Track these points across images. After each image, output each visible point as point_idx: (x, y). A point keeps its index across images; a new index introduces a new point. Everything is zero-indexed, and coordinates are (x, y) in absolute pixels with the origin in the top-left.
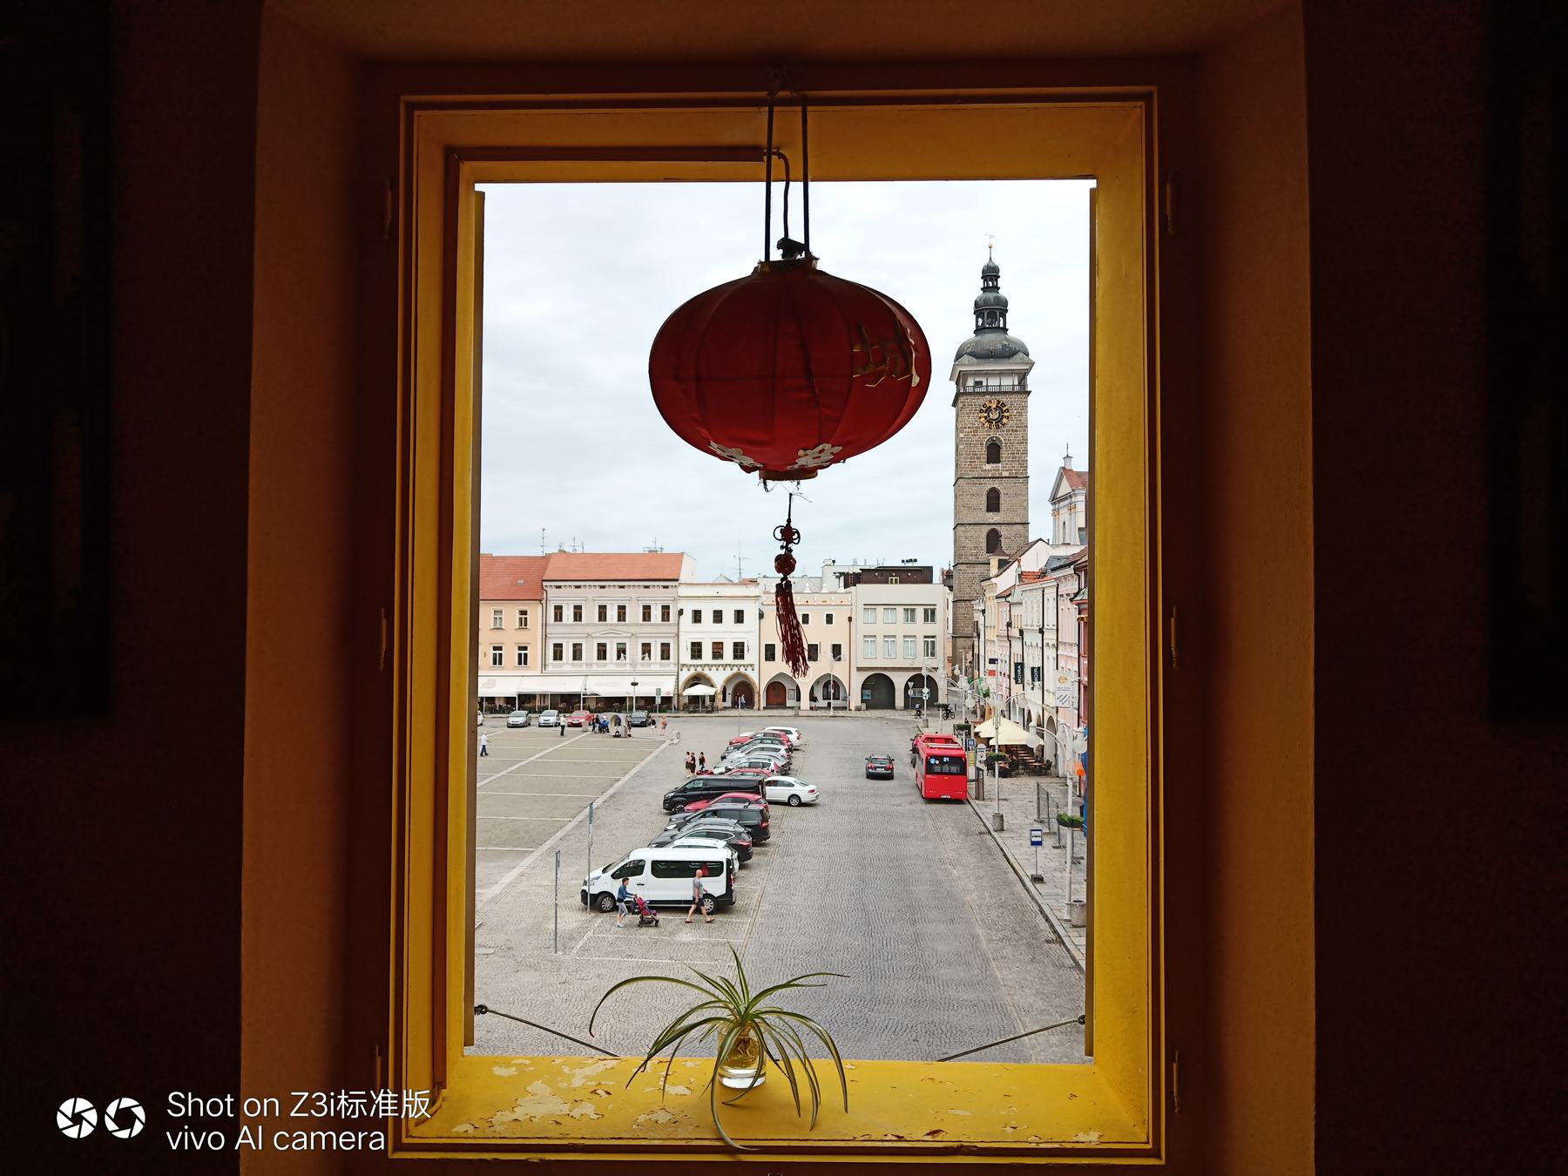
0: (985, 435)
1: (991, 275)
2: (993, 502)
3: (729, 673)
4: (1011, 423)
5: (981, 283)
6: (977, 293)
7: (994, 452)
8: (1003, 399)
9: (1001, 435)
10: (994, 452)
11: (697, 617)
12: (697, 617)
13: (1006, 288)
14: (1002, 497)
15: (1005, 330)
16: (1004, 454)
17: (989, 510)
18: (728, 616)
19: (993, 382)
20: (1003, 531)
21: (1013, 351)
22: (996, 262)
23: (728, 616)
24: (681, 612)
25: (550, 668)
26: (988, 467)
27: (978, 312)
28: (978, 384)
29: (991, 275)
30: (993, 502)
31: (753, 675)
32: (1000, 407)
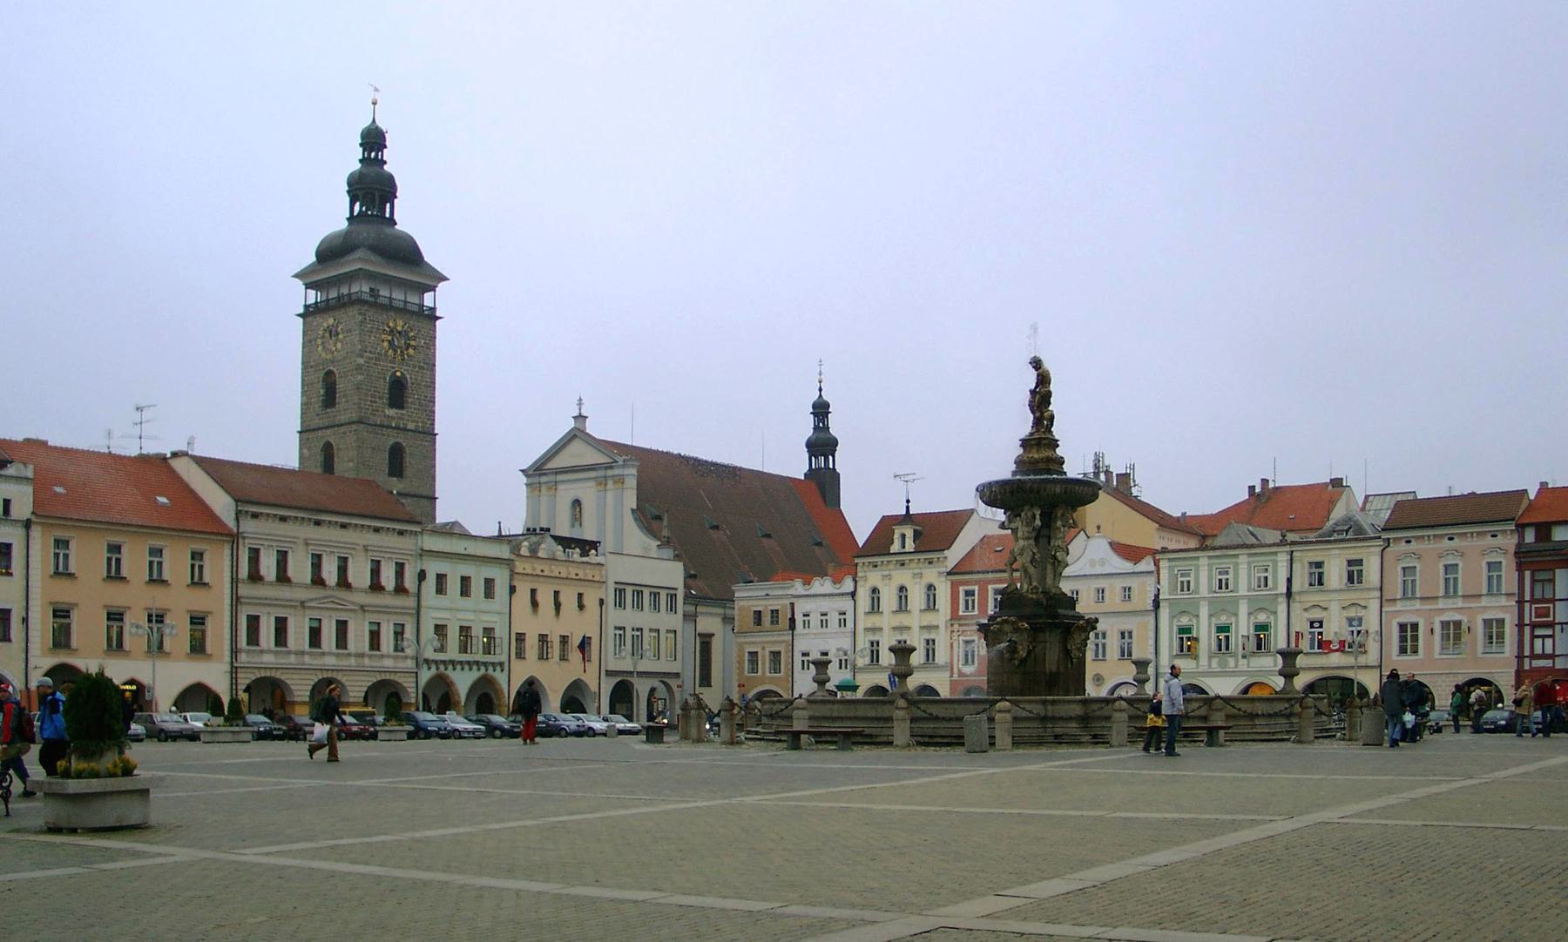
1: (373, 140)
3: (473, 675)
7: (398, 393)
11: (441, 589)
12: (441, 589)
13: (394, 161)
14: (407, 459)
15: (392, 222)
17: (391, 474)
18: (477, 587)
19: (398, 295)
21: (407, 254)
22: (379, 123)
23: (477, 587)
24: (422, 576)
25: (243, 657)
26: (392, 412)
31: (500, 677)
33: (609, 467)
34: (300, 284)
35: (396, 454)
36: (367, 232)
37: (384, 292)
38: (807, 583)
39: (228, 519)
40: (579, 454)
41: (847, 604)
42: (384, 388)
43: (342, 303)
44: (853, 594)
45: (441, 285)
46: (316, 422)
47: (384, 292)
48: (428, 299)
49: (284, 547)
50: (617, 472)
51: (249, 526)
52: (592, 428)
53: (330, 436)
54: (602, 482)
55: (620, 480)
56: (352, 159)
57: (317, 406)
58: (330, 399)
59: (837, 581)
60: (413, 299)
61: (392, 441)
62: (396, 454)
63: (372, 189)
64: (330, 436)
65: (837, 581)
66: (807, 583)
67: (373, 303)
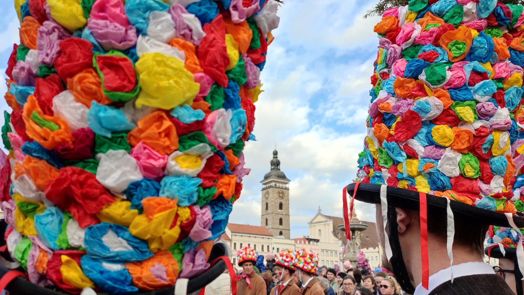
0: (279, 201)
1: (275, 153)
2: (281, 222)
4: (286, 198)
5: (272, 156)
6: (272, 159)
7: (281, 206)
8: (284, 190)
9: (283, 202)
10: (281, 206)
13: (280, 157)
15: (279, 169)
16: (284, 207)
19: (281, 185)
20: (284, 232)
21: (283, 177)
22: (277, 150)
24: (273, 248)
26: (280, 211)
27: (272, 163)
28: (276, 185)
29: (275, 153)
30: (281, 222)
32: (283, 193)
33: (326, 221)
34: (261, 184)
35: (281, 220)
36: (275, 172)
37: (278, 185)
38: (368, 249)
39: (230, 237)
40: (320, 218)
41: (377, 254)
42: (278, 205)
43: (269, 187)
44: (378, 252)
45: (290, 182)
46: (264, 214)
47: (278, 185)
48: (287, 186)
49: (249, 243)
50: (328, 222)
51: (234, 237)
52: (322, 212)
53: (267, 216)
54: (325, 225)
55: (329, 225)
56: (271, 157)
57: (264, 210)
58: (267, 209)
59: (375, 248)
60: (284, 186)
61: (280, 217)
62: (281, 220)
63: (276, 164)
64: (267, 216)
65: (375, 248)
66: (368, 249)
67: (276, 187)
